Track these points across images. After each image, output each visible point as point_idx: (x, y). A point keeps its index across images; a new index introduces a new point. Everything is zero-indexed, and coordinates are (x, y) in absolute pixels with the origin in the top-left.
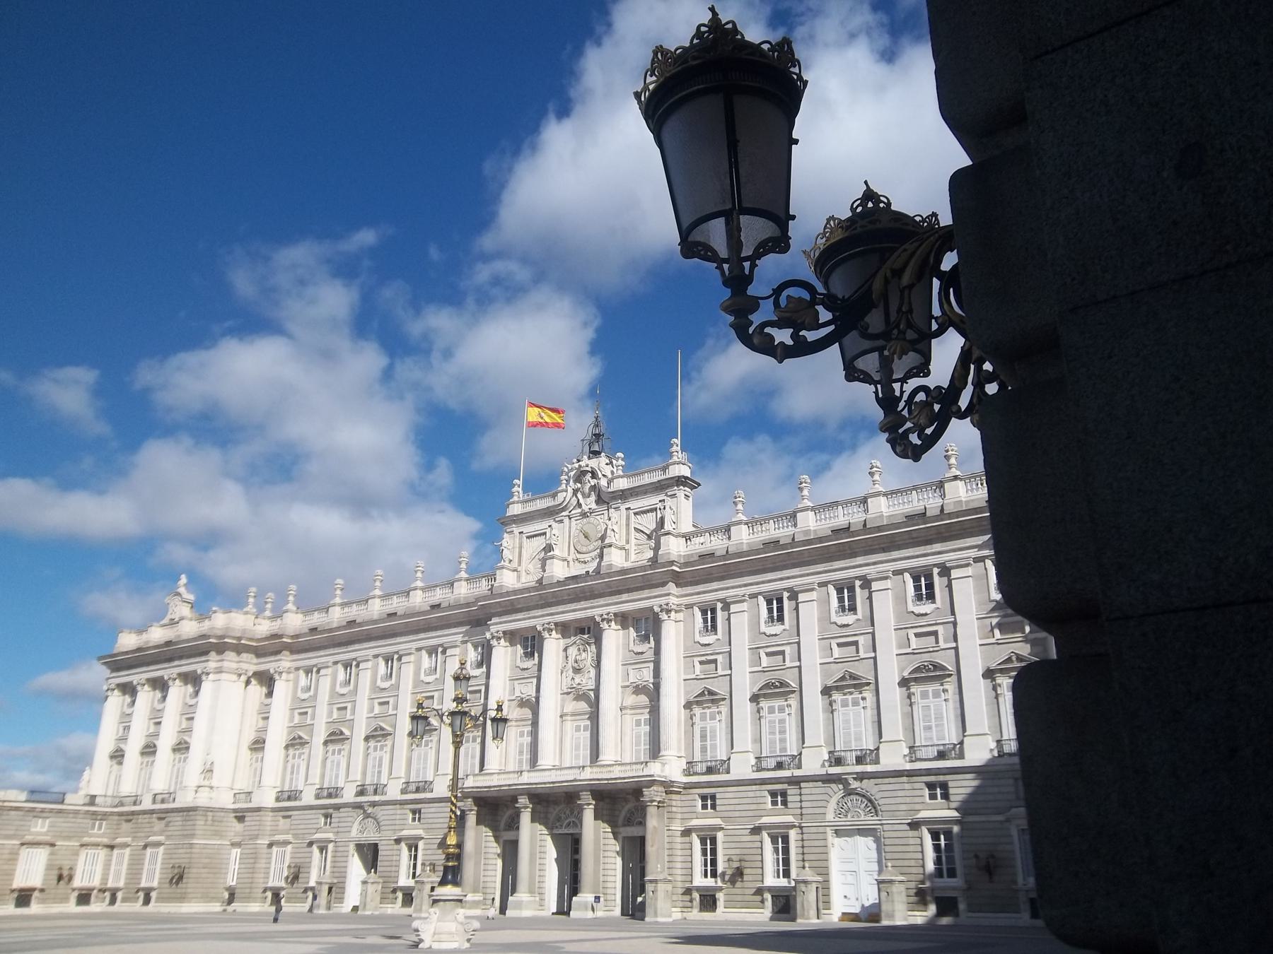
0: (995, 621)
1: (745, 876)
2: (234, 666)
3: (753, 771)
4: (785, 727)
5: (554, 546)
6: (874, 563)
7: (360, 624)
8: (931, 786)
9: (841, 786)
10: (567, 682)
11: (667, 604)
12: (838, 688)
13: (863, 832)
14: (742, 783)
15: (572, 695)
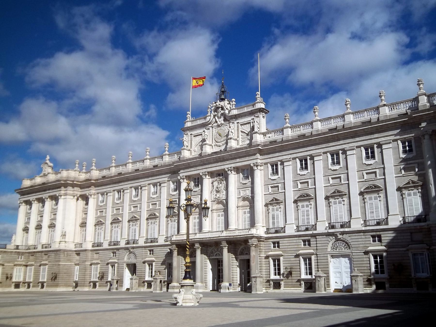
0: (402, 167)
1: (292, 275)
2: (72, 192)
3: (295, 232)
4: (309, 213)
5: (206, 139)
6: (348, 143)
7: (124, 174)
8: (373, 237)
9: (334, 237)
10: (213, 196)
11: (257, 163)
12: (332, 197)
13: (344, 256)
14: (291, 237)
15: (216, 202)
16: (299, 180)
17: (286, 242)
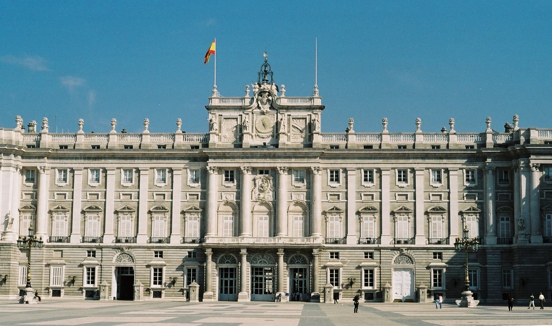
0: (465, 194)
7: (102, 150)
9: (399, 252)
11: (318, 167)
13: (405, 269)
16: (363, 192)
17: (347, 253)
